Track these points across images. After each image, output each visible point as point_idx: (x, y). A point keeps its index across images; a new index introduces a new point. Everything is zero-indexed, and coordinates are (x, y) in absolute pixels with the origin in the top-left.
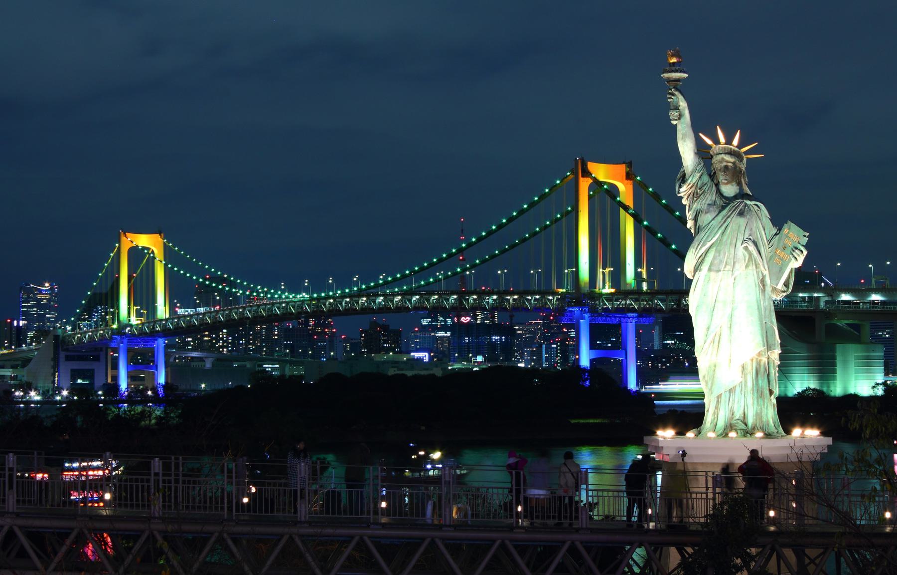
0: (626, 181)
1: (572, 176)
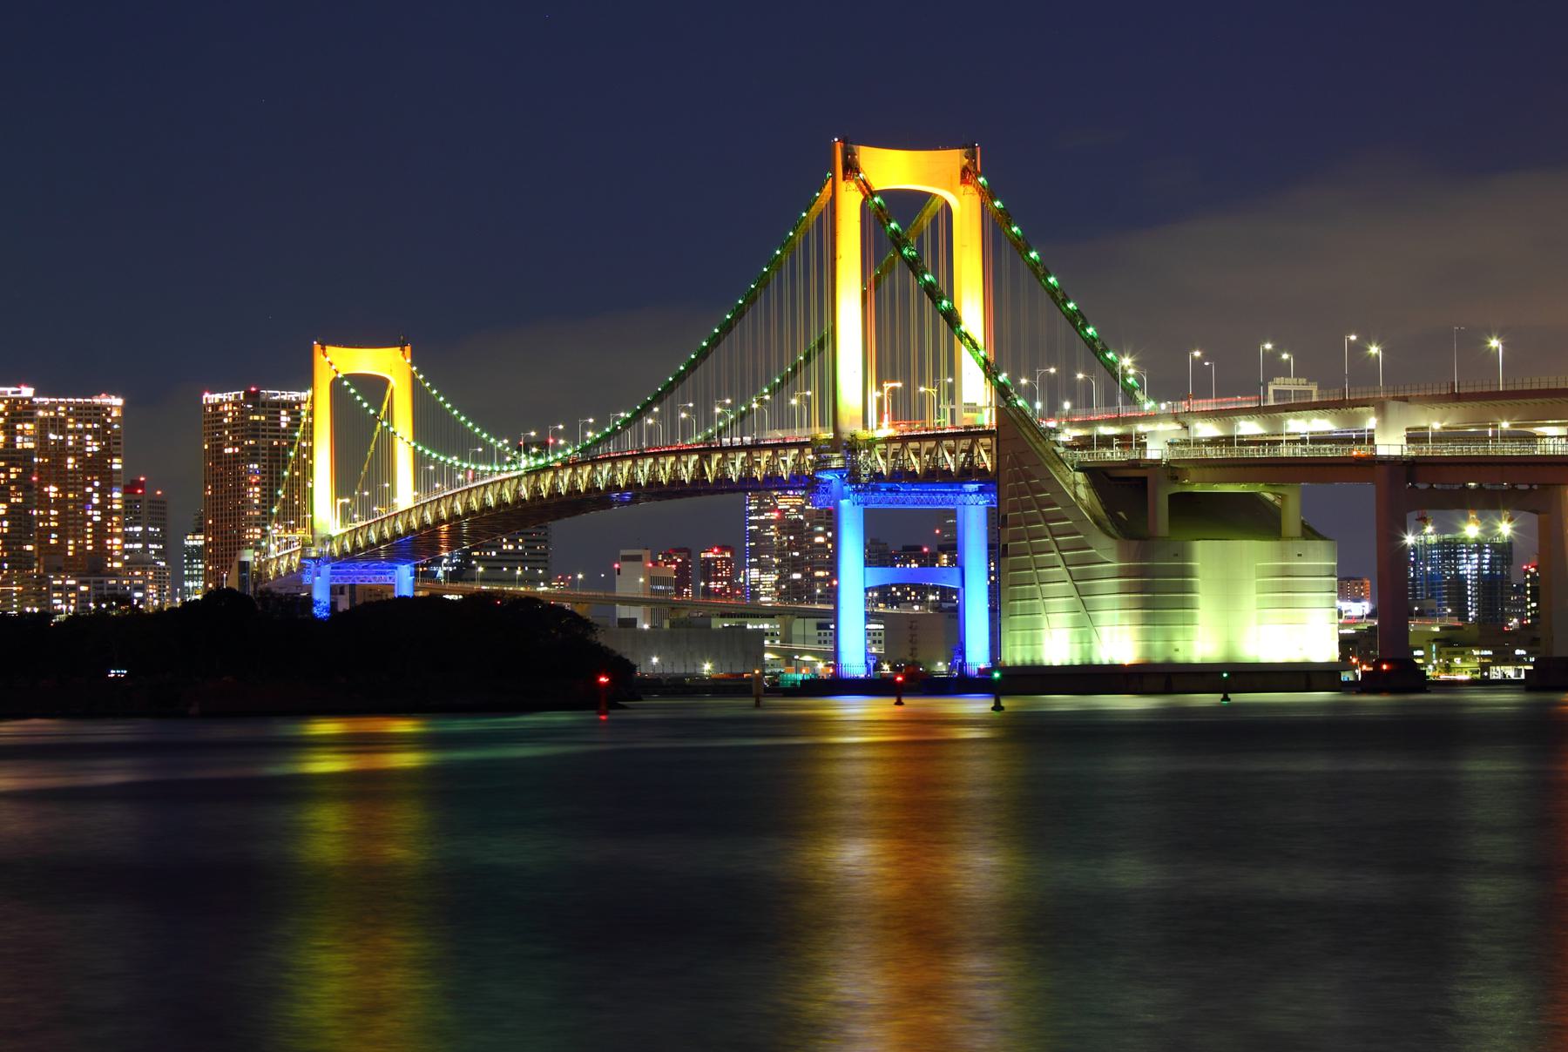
0: (961, 189)
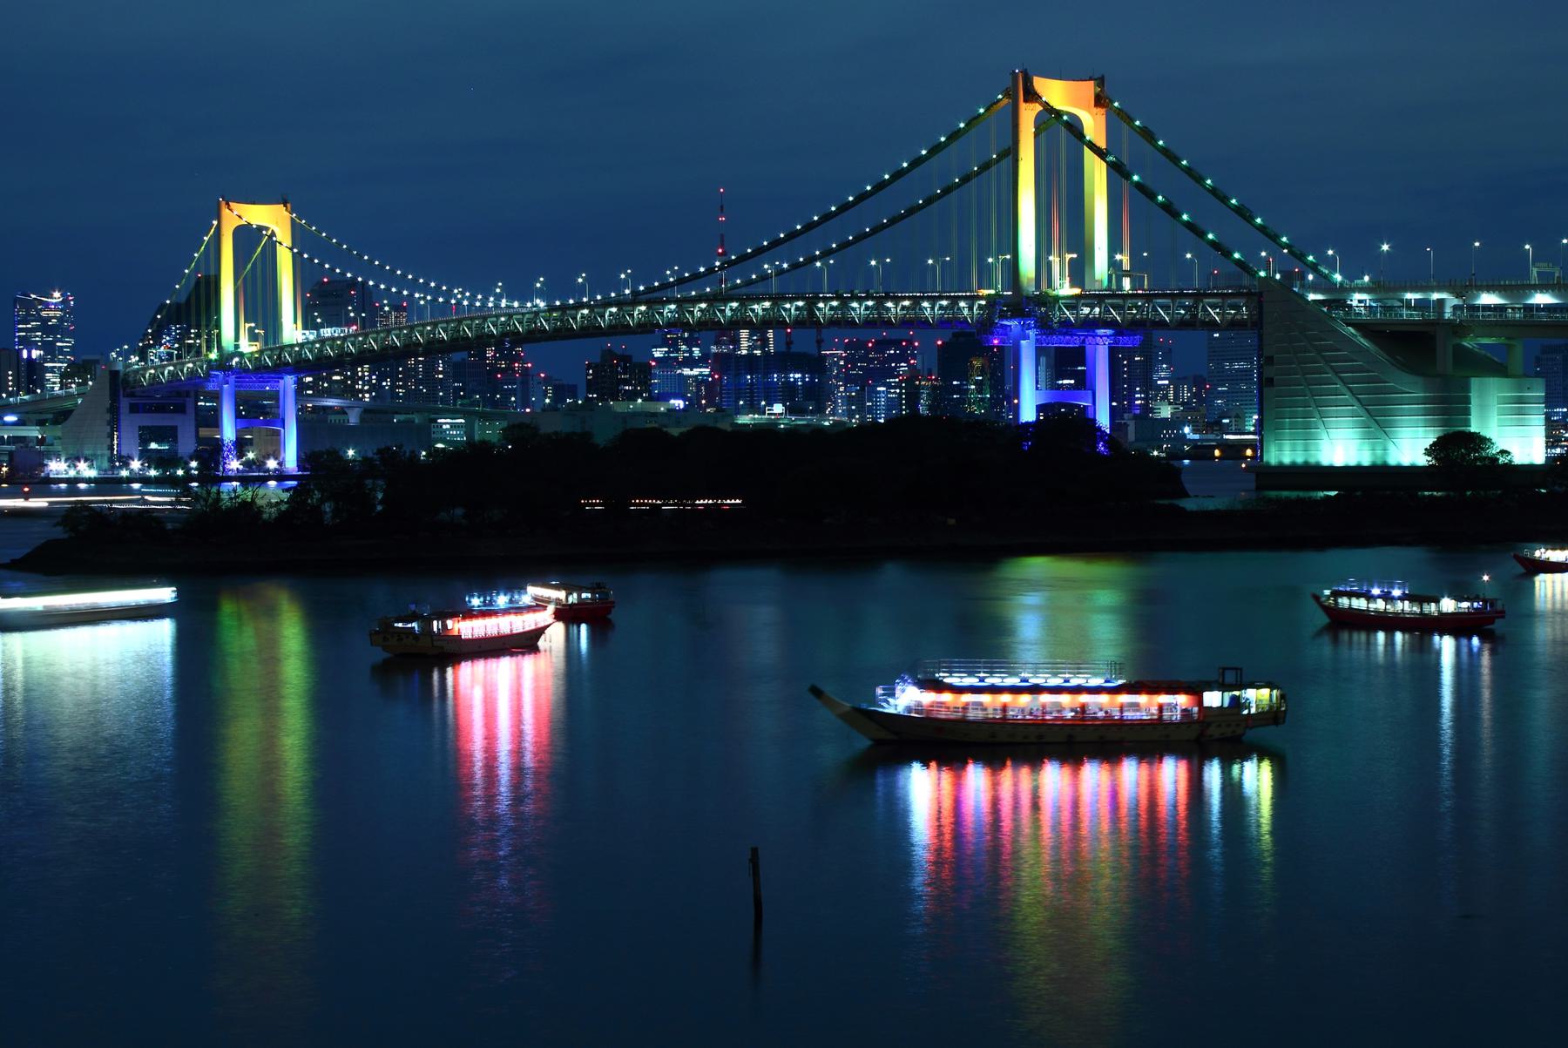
0: (1096, 110)
1: (1006, 101)
